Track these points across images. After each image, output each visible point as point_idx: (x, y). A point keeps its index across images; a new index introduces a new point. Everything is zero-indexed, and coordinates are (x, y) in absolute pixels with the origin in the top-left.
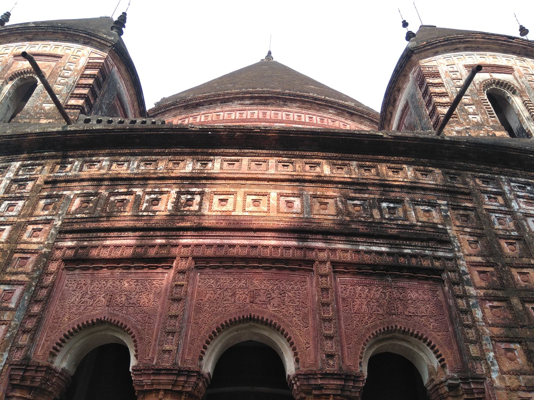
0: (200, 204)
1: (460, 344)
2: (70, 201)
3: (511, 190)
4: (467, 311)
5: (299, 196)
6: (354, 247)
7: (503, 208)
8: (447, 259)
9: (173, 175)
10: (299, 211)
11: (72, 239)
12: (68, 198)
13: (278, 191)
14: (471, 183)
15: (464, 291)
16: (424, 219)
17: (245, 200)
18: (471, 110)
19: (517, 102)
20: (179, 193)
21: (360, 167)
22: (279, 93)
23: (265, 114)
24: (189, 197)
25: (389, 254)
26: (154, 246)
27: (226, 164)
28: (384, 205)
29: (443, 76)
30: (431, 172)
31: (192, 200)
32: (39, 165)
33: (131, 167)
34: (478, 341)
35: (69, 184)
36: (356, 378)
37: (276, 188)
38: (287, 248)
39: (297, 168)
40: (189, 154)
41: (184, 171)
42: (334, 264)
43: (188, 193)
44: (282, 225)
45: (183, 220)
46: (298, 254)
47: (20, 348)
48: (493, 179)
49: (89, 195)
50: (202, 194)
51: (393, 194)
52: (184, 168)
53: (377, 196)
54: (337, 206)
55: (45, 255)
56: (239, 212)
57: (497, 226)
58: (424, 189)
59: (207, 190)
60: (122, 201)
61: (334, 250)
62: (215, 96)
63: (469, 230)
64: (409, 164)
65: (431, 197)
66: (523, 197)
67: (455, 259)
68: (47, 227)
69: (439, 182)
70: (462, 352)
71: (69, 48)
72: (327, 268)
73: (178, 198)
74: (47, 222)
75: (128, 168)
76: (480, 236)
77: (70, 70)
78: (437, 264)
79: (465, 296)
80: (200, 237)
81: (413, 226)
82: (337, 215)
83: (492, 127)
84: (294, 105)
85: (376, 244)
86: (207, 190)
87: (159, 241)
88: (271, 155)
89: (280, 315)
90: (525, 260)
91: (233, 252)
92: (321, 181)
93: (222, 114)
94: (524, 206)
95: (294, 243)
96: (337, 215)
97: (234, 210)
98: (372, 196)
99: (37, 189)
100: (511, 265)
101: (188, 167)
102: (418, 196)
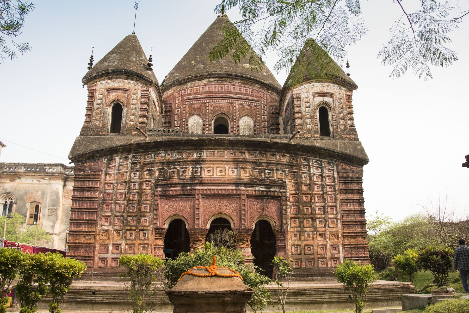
0: (201, 172)
1: (281, 219)
2: (155, 172)
3: (313, 164)
4: (286, 210)
5: (237, 168)
6: (254, 189)
8: (283, 192)
9: (189, 160)
11: (160, 188)
12: (154, 171)
13: (229, 166)
14: (299, 161)
15: (286, 204)
16: (279, 177)
18: (308, 122)
19: (330, 114)
20: (193, 168)
21: (260, 154)
25: (265, 191)
26: (187, 190)
27: (208, 153)
28: (267, 171)
29: (301, 100)
30: (286, 156)
31: (197, 170)
32: (139, 155)
33: (173, 156)
34: (286, 219)
35: (153, 165)
36: (251, 230)
37: (228, 164)
38: (232, 190)
39: (236, 155)
40: (194, 149)
42: (247, 195)
43: (196, 168)
44: (230, 181)
45: (196, 180)
46: (235, 192)
48: (307, 159)
50: (201, 168)
51: (270, 166)
52: (193, 156)
53: (264, 168)
55: (153, 194)
56: (215, 176)
57: (304, 179)
58: (282, 164)
59: (203, 166)
61: (247, 191)
63: (293, 181)
64: (278, 152)
65: (284, 167)
66: (316, 167)
67: (285, 193)
68: (150, 183)
69: (288, 161)
70: (282, 222)
71: (130, 83)
73: (192, 170)
74: (150, 181)
76: (296, 184)
77: (135, 99)
78: (280, 194)
79: (286, 205)
80: (202, 186)
81: (275, 180)
82: (249, 176)
83: (315, 132)
85: (261, 187)
86: (203, 166)
88: (226, 149)
90: (308, 192)
92: (245, 161)
94: (314, 170)
95: (234, 188)
96: (249, 176)
97: (213, 175)
98: (263, 168)
99: (142, 167)
100: (303, 194)
101: (195, 155)
102: (279, 167)
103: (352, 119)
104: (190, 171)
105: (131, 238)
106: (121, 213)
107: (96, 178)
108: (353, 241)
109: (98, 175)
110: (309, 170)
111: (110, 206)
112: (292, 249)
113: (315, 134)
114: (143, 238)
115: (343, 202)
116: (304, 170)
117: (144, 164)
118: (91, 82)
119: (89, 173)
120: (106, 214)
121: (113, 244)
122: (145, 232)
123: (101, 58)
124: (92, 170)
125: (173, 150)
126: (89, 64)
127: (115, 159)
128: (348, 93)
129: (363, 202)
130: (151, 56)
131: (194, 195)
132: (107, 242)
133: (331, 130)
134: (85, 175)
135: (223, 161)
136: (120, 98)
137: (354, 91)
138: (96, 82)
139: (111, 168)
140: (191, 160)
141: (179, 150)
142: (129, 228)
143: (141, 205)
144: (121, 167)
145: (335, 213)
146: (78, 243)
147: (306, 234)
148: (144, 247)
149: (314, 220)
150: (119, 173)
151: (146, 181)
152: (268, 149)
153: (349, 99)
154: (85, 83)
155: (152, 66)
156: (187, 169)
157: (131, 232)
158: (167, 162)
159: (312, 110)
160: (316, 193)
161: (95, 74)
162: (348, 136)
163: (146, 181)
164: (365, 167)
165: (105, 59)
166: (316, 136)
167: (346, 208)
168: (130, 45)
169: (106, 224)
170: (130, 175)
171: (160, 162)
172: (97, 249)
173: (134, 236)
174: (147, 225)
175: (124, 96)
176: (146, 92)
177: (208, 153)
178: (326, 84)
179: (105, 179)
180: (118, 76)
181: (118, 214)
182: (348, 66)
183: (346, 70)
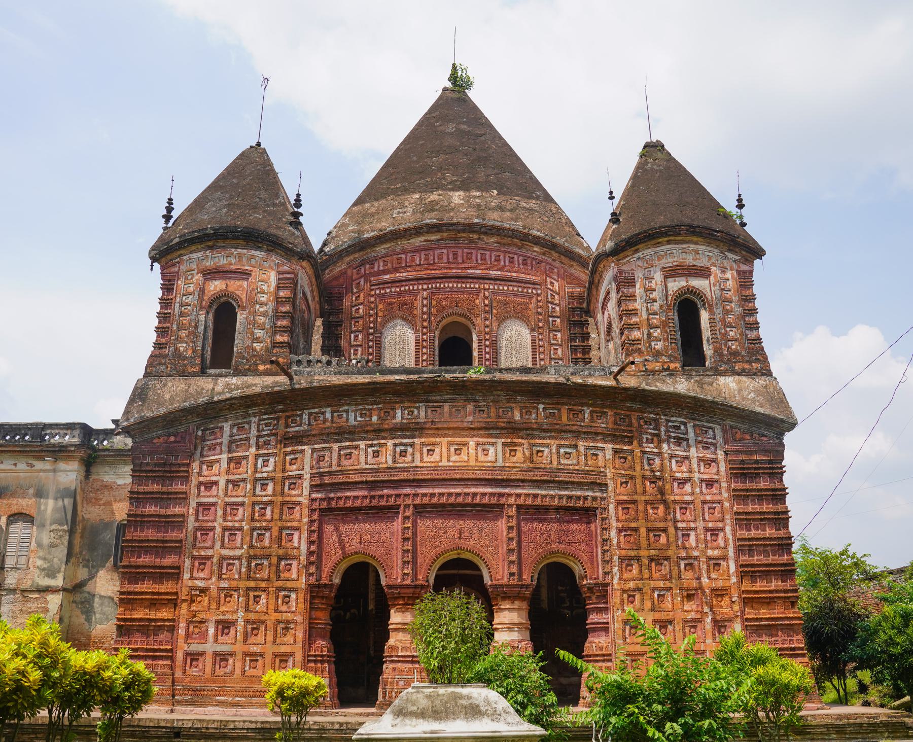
0: (413, 454)
3: (667, 431)
7: (655, 450)
9: (386, 426)
10: (493, 459)
13: (476, 439)
17: (449, 450)
19: (704, 316)
20: (395, 445)
24: (403, 448)
41: (394, 421)
42: (519, 507)
44: (480, 475)
46: (494, 501)
47: (311, 574)
52: (394, 418)
54: (524, 454)
56: (444, 463)
59: (417, 441)
60: (350, 454)
72: (513, 511)
77: (264, 293)
82: (524, 462)
83: (669, 356)
84: (491, 240)
89: (478, 547)
93: (403, 256)
103: (755, 326)
107: (179, 472)
108: (764, 613)
109: (184, 465)
112: (624, 631)
113: (672, 361)
115: (740, 519)
118: (169, 257)
120: (203, 553)
121: (218, 622)
123: (190, 201)
126: (164, 216)
127: (221, 428)
128: (744, 267)
129: (788, 519)
130: (298, 195)
131: (398, 507)
132: (202, 616)
133: (708, 350)
135: (463, 429)
136: (231, 289)
137: (757, 262)
138: (180, 255)
140: (392, 426)
145: (722, 545)
146: (140, 620)
147: (656, 595)
152: (564, 400)
153: (746, 280)
154: (154, 259)
155: (301, 218)
156: (384, 450)
159: (661, 307)
160: (677, 498)
161: (177, 240)
162: (747, 366)
165: (199, 204)
166: (672, 366)
167: (745, 534)
168: (252, 173)
169: (202, 575)
172: (182, 632)
174: (294, 576)
175: (241, 286)
176: (288, 276)
177: (429, 411)
178: (692, 247)
179: (200, 474)
180: (228, 242)
182: (740, 206)
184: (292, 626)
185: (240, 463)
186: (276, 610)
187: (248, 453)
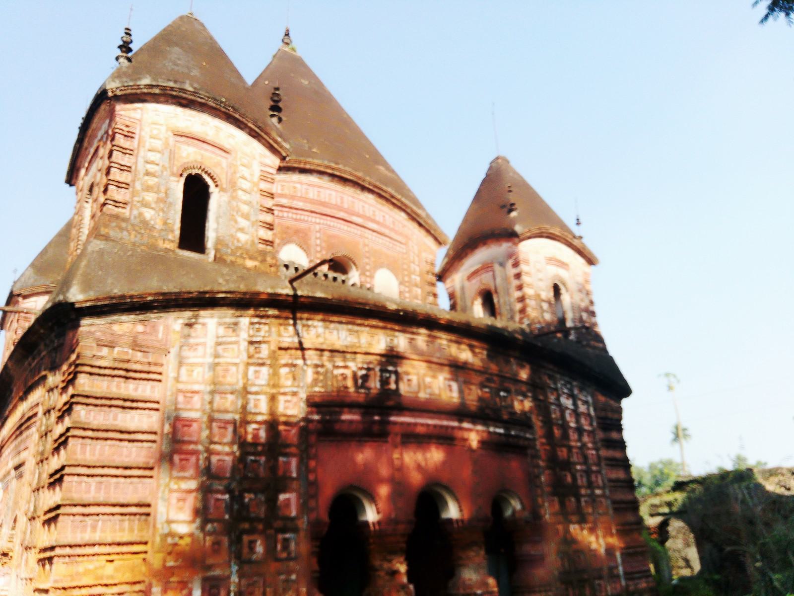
22: (359, 178)
23: (342, 198)
24: (388, 375)
28: (502, 394)
32: (265, 324)
49: (317, 366)
62: (296, 162)
67: (534, 440)
68: (295, 399)
71: (232, 136)
73: (381, 376)
74: (295, 394)
75: (339, 338)
79: (538, 466)
87: (377, 418)
91: (420, 430)
99: (273, 356)
104: (378, 378)
105: (254, 557)
106: (225, 482)
107: (149, 372)
110: (558, 399)
111: (193, 459)
114: (284, 555)
116: (552, 398)
117: (280, 349)
119: (130, 353)
122: (287, 536)
124: (136, 345)
125: (340, 323)
134: (115, 360)
139: (192, 347)
141: (353, 324)
142: (246, 526)
143: (277, 460)
144: (220, 348)
148: (287, 581)
149: (578, 501)
150: (217, 364)
151: (284, 394)
156: (372, 373)
157: (252, 538)
158: (331, 351)
163: (284, 394)
164: (625, 403)
170: (246, 374)
171: (317, 349)
173: (260, 548)
174: (294, 514)
179: (177, 380)
181: (218, 486)
182: (578, 224)
183: (576, 231)
184: (294, 577)
185: (227, 370)
186: (278, 560)
187: (237, 361)
